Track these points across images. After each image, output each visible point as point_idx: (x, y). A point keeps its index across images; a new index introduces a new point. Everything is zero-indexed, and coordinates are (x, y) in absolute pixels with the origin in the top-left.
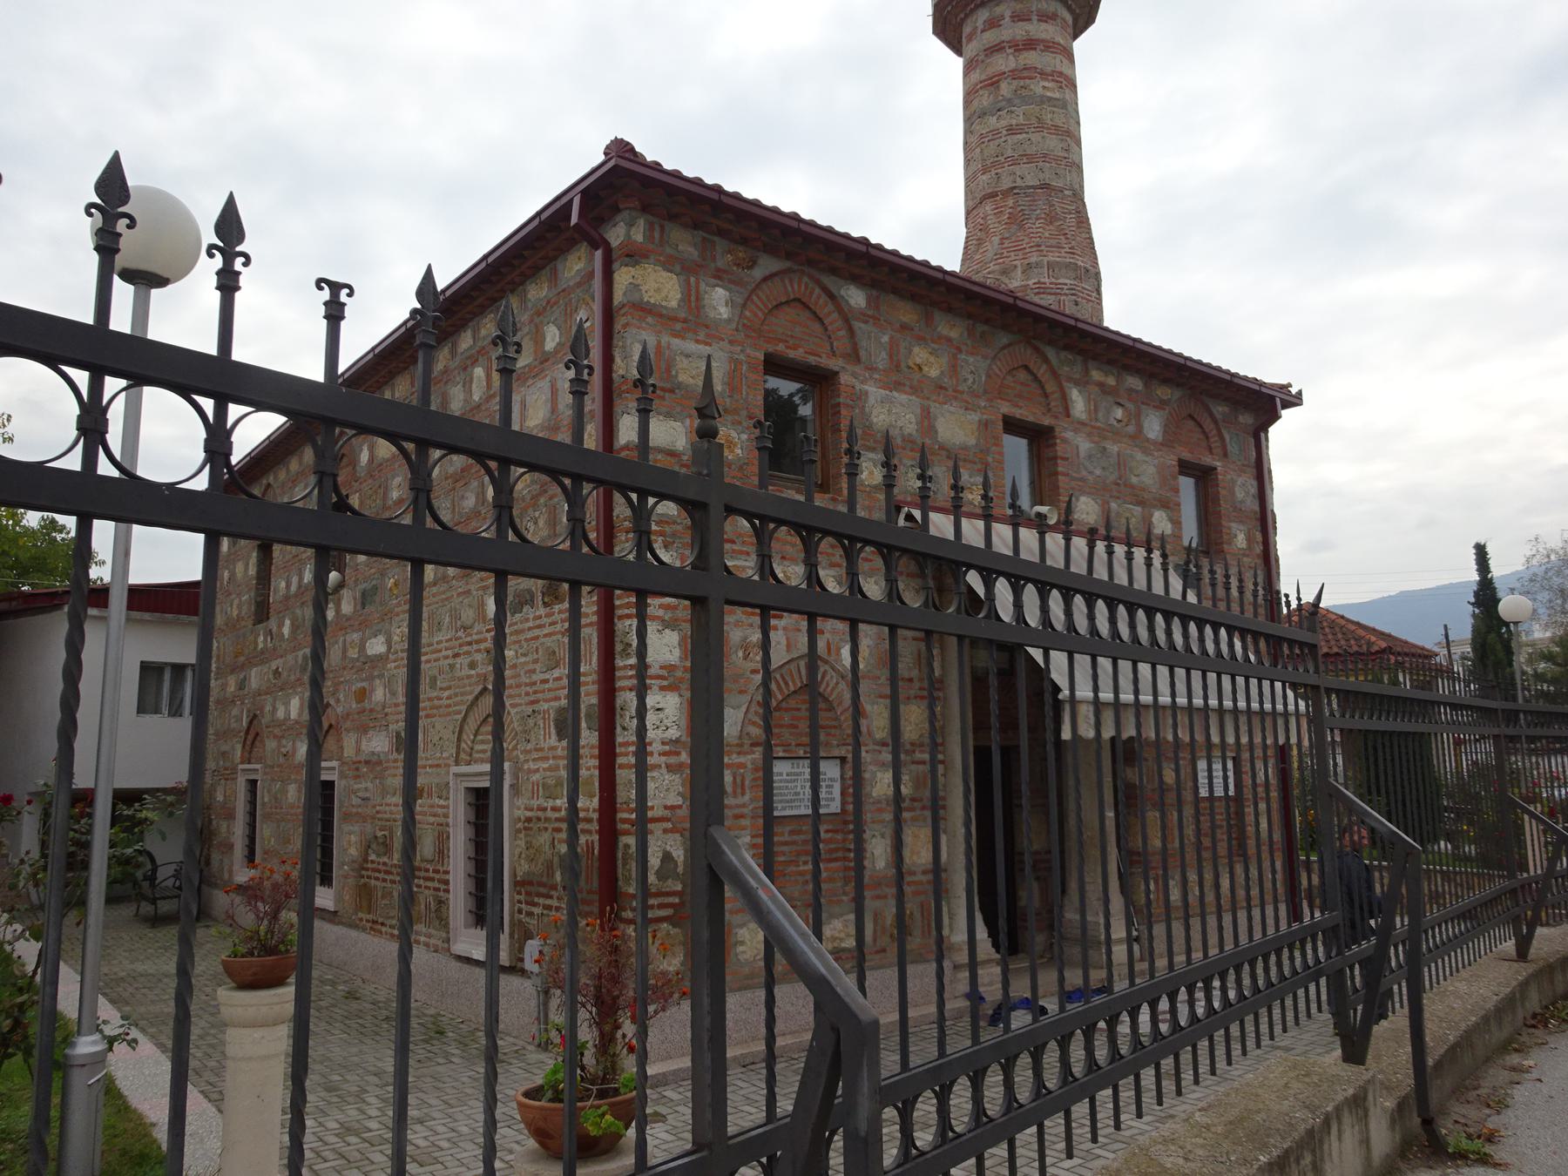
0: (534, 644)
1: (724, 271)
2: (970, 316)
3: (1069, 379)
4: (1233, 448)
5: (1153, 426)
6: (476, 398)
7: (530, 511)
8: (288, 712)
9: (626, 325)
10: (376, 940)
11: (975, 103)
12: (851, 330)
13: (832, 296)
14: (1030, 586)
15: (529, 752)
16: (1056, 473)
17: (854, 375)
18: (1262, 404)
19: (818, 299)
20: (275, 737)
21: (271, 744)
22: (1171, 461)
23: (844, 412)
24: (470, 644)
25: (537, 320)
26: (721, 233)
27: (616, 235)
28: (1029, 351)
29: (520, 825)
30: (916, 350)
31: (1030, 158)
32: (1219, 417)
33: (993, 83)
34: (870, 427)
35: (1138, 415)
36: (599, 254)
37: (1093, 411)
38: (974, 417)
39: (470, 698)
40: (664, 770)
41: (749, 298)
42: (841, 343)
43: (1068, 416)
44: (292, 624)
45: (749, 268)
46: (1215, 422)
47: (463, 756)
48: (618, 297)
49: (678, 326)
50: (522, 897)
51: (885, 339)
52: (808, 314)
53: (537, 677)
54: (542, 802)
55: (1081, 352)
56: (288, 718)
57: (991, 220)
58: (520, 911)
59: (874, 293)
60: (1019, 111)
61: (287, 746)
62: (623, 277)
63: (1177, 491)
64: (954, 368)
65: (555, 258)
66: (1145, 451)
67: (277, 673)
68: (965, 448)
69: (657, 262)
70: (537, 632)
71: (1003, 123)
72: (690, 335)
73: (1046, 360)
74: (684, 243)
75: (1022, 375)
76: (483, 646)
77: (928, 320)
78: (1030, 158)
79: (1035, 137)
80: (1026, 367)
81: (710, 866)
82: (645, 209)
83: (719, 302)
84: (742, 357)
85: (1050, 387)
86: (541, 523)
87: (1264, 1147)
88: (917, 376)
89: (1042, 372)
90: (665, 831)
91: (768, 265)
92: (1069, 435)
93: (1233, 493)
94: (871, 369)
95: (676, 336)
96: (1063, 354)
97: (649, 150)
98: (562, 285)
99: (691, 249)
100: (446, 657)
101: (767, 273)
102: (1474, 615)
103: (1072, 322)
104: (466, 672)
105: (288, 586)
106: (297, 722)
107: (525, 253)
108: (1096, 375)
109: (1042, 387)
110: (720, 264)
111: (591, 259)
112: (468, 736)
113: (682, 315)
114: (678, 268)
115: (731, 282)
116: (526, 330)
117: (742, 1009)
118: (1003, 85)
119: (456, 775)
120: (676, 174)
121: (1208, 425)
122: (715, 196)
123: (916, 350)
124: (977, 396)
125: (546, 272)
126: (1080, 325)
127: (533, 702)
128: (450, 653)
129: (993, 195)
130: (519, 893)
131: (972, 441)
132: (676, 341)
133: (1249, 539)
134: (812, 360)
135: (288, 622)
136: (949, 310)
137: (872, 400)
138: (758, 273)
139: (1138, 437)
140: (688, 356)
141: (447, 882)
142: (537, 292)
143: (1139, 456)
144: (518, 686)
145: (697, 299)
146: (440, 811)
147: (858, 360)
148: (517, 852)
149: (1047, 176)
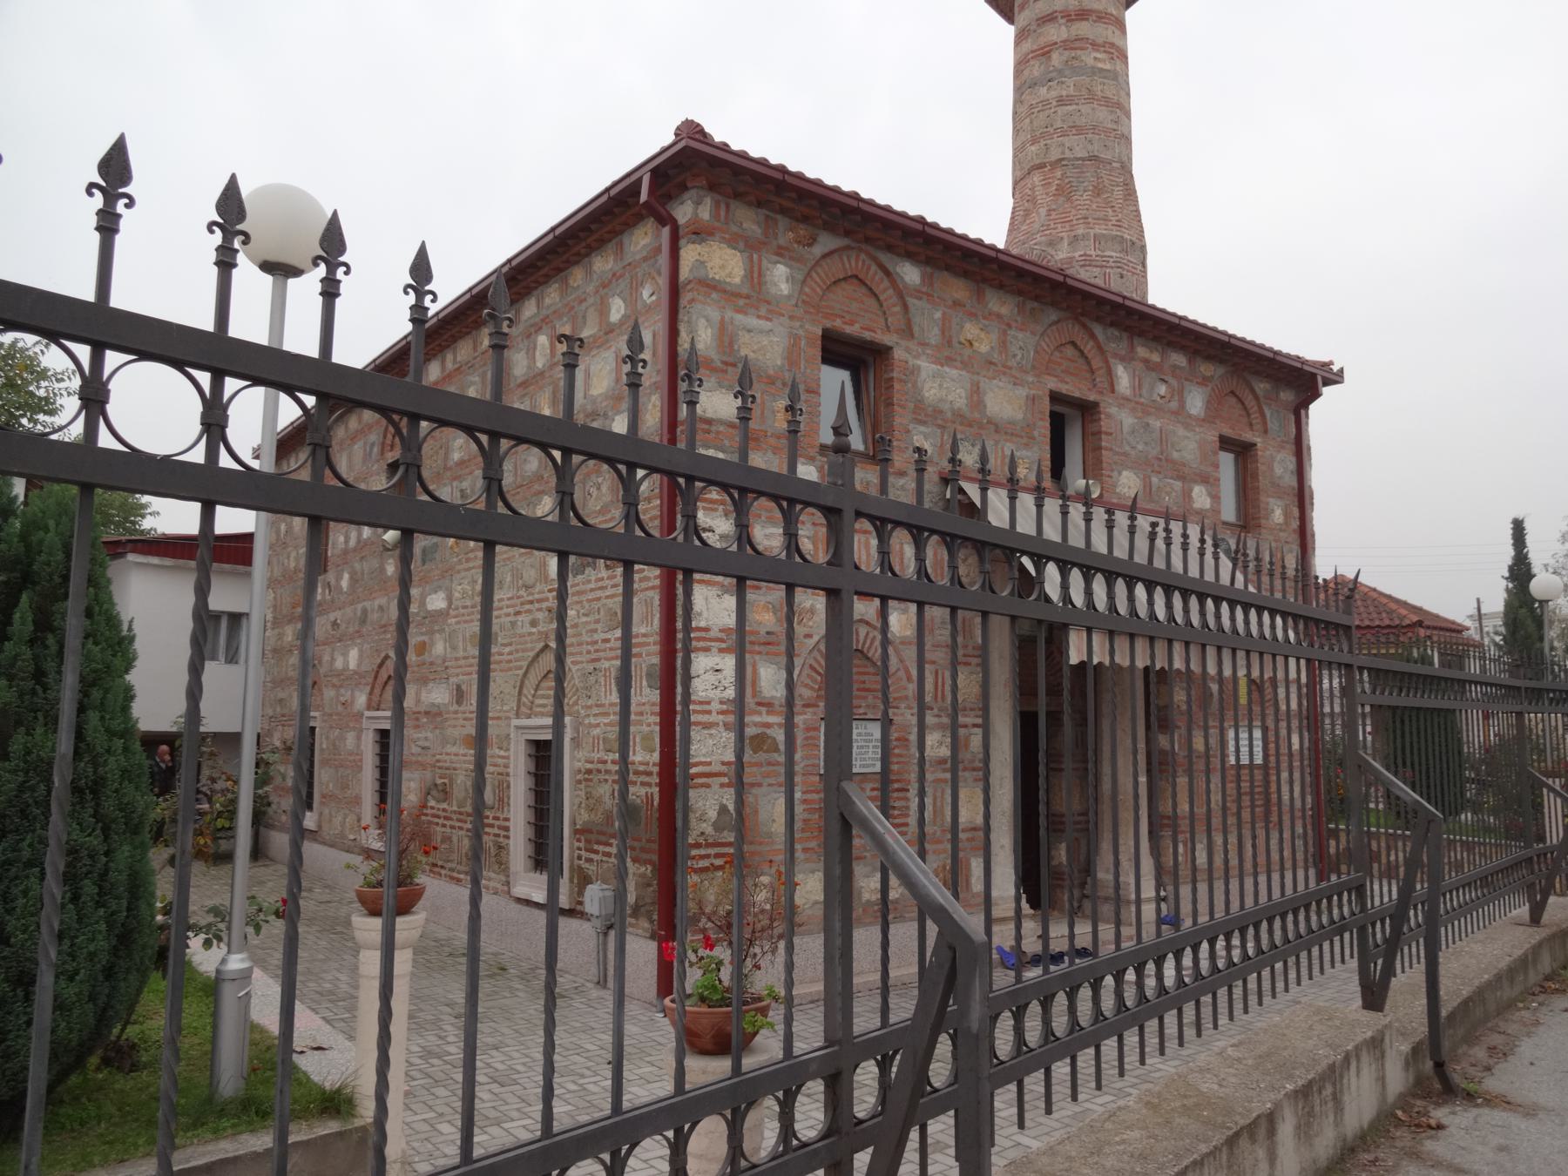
0: (596, 605)
1: (787, 249)
2: (1020, 293)
3: (1116, 356)
4: (1273, 425)
5: (1196, 402)
6: (539, 364)
7: (593, 477)
8: (346, 663)
9: (693, 300)
10: (436, 882)
11: (1026, 73)
12: (905, 307)
13: (887, 273)
14: (1099, 576)
15: (590, 707)
16: (1100, 448)
17: (908, 350)
18: (1302, 381)
19: (874, 275)
20: (334, 686)
21: (329, 693)
22: (1212, 437)
23: (897, 386)
24: (531, 602)
25: (602, 292)
26: (783, 211)
27: (683, 212)
28: (1077, 327)
29: (579, 777)
30: (968, 326)
31: (1079, 130)
32: (1260, 393)
33: (1045, 53)
34: (921, 401)
35: (1181, 393)
36: (666, 231)
37: (1137, 387)
38: (1022, 392)
39: (532, 654)
40: (721, 729)
41: (808, 274)
42: (896, 319)
43: (1113, 391)
44: (351, 578)
45: (810, 245)
46: (1256, 398)
47: (523, 709)
48: (685, 273)
49: (741, 302)
50: (582, 845)
51: (938, 315)
52: (864, 289)
53: (599, 636)
54: (602, 755)
55: (1127, 329)
56: (346, 668)
57: (1039, 191)
58: (579, 858)
59: (929, 270)
60: (1070, 82)
61: (346, 695)
62: (690, 254)
63: (1217, 466)
64: (1003, 344)
65: (622, 232)
66: (1187, 426)
67: (335, 624)
68: (1011, 423)
69: (723, 240)
70: (599, 594)
71: (1054, 94)
72: (752, 311)
73: (1093, 336)
74: (748, 220)
75: (1070, 352)
76: (544, 605)
77: (980, 295)
78: (1079, 130)
79: (1085, 109)
80: (1073, 344)
81: (842, 815)
82: (712, 187)
83: (780, 278)
84: (801, 332)
85: (1097, 363)
86: (604, 489)
87: (1290, 1077)
88: (967, 352)
89: (1089, 348)
90: (722, 785)
91: (827, 242)
92: (1113, 410)
93: (1271, 469)
94: (923, 344)
95: (738, 311)
97: (719, 132)
98: (628, 259)
99: (754, 227)
100: (508, 615)
101: (826, 250)
102: (1507, 590)
103: (1120, 300)
104: (528, 629)
105: (347, 541)
106: (355, 672)
107: (593, 227)
108: (1142, 351)
109: (1088, 363)
110: (782, 241)
111: (658, 236)
112: (529, 690)
113: (745, 291)
114: (741, 245)
115: (791, 258)
116: (591, 300)
117: (865, 940)
118: (1055, 55)
119: (518, 728)
120: (743, 155)
121: (1250, 401)
122: (779, 176)
123: (968, 326)
124: (1026, 372)
125: (611, 246)
126: (1128, 303)
127: (594, 660)
128: (511, 610)
129: (1041, 166)
130: (579, 840)
131: (1020, 416)
132: (739, 317)
133: (1286, 514)
134: (867, 335)
135: (346, 576)
136: (1001, 287)
137: (923, 374)
138: (817, 250)
139: (1180, 413)
140: (749, 331)
141: (507, 829)
142: (603, 264)
143: (1181, 431)
144: (580, 644)
145: (760, 275)
146: (500, 761)
147: (912, 336)
148: (577, 801)
149: (1096, 148)
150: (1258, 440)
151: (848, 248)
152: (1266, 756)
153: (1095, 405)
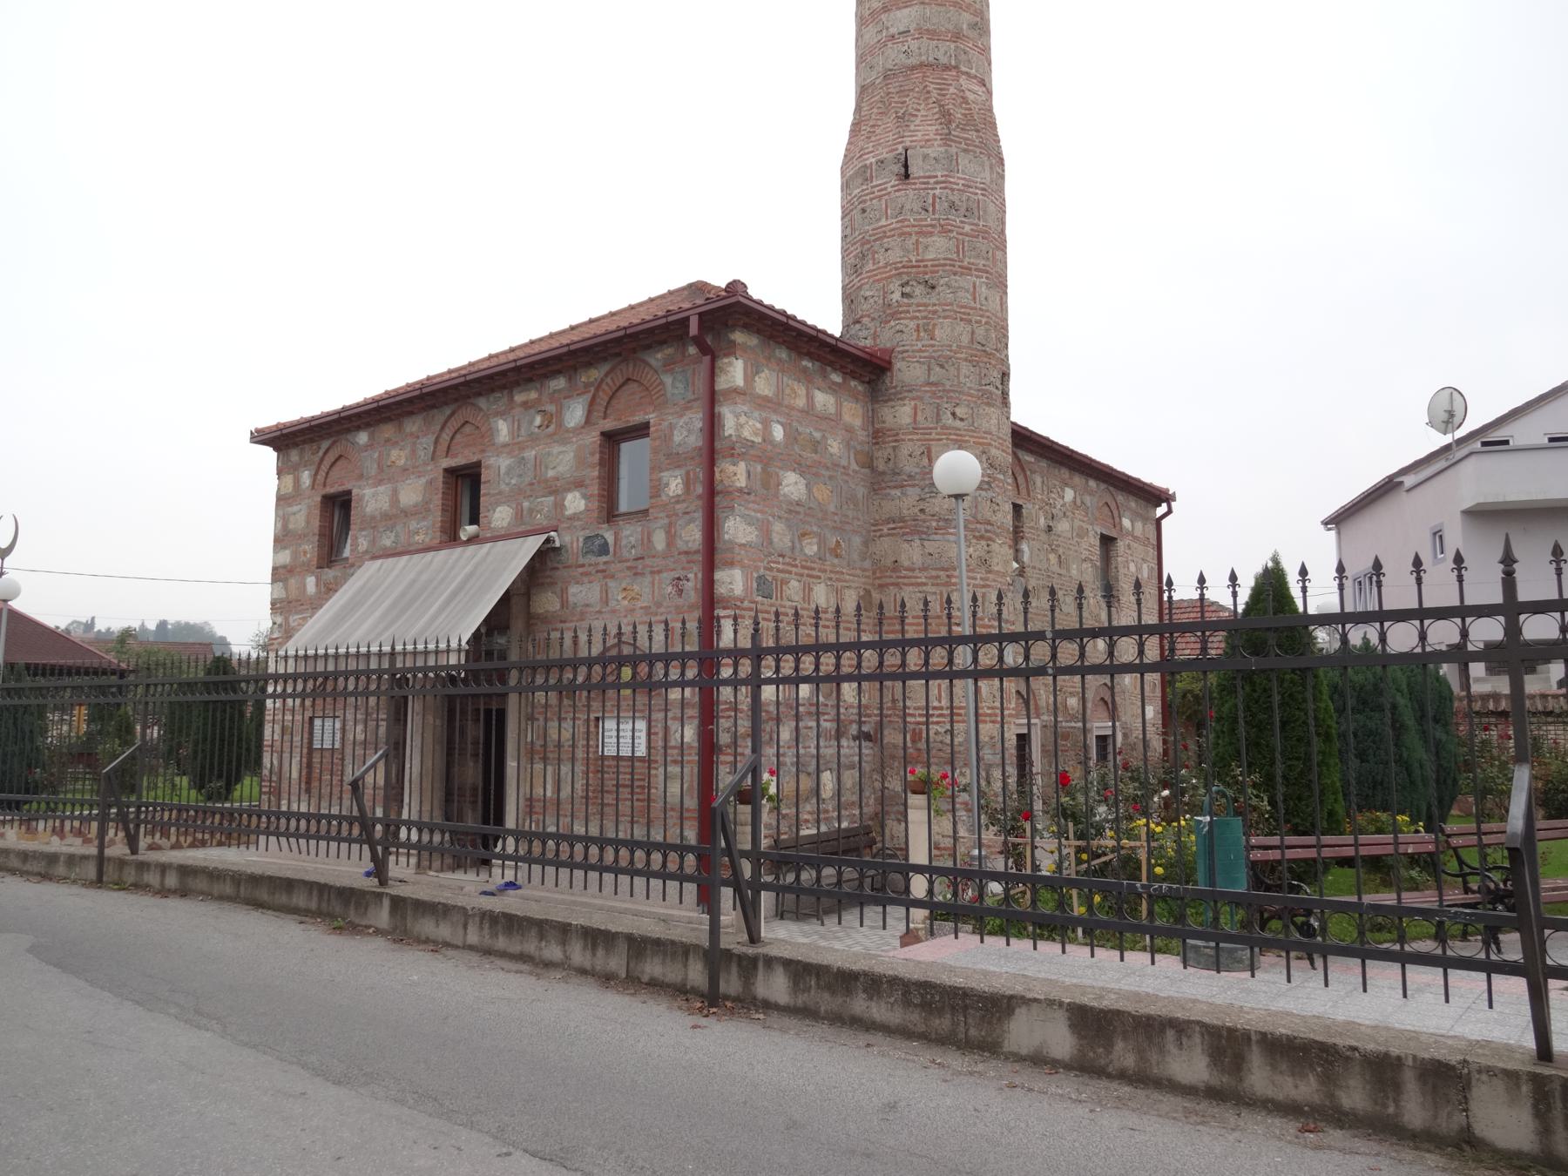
22: (592, 438)
26: (304, 442)
55: (504, 387)
64: (414, 452)
66: (564, 442)
75: (468, 429)
77: (400, 428)
91: (325, 444)
92: (492, 461)
108: (519, 398)
133: (687, 484)
134: (341, 489)
143: (556, 449)
150: (652, 417)
151: (334, 443)
152: (649, 747)
153: (478, 464)
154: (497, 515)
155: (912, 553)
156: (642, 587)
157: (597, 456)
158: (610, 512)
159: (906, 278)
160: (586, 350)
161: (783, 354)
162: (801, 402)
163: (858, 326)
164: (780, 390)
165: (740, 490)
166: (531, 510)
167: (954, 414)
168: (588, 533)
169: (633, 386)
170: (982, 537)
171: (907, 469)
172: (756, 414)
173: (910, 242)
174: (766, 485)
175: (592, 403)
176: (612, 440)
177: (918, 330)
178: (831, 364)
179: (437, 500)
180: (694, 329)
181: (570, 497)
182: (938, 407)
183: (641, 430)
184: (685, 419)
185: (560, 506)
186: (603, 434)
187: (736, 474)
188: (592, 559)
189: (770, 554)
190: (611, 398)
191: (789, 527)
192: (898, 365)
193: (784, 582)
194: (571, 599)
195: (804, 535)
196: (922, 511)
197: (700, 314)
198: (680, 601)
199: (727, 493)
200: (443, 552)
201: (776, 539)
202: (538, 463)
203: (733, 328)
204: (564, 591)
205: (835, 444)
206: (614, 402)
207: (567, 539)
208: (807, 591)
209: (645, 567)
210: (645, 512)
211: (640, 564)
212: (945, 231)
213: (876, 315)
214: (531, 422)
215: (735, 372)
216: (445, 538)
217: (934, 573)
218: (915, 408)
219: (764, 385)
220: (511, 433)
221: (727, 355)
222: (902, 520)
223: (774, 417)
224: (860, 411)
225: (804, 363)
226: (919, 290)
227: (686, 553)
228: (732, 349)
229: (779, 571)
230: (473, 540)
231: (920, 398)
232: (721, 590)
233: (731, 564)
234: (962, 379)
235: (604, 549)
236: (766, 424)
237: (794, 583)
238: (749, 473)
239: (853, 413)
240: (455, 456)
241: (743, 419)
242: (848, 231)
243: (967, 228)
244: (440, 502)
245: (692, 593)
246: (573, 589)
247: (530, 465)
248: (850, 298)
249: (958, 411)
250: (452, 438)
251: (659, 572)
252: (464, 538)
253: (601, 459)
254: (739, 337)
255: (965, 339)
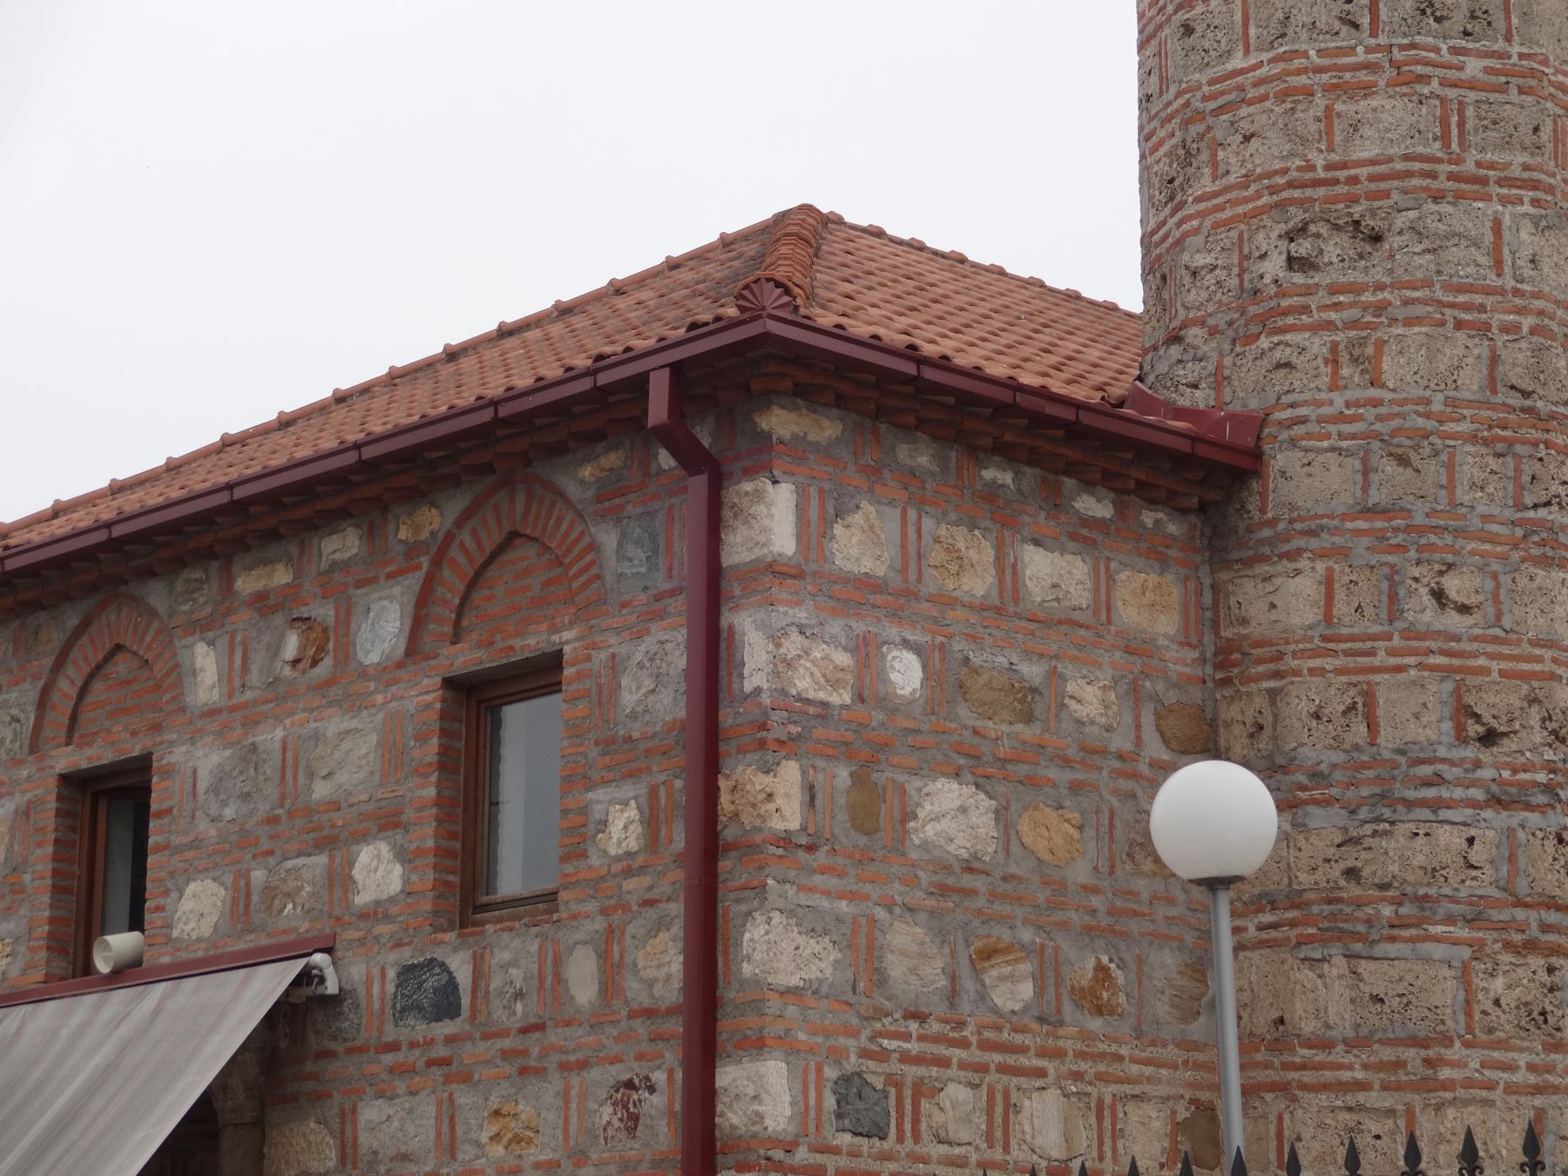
22: (421, 695)
66: (353, 704)
73: (153, 614)
75: (122, 667)
92: (177, 755)
96: (179, 586)
108: (247, 584)
133: (652, 822)
143: (335, 723)
150: (568, 639)
153: (143, 765)
154: (186, 905)
155: (1325, 996)
156: (538, 1105)
157: (435, 742)
158: (465, 888)
159: (1297, 216)
160: (408, 458)
161: (920, 456)
162: (979, 583)
163: (1175, 351)
164: (910, 556)
165: (785, 840)
166: (270, 891)
167: (1439, 595)
168: (407, 956)
169: (525, 554)
170: (1531, 946)
171: (1308, 755)
172: (835, 627)
173: (1308, 117)
174: (865, 821)
175: (423, 600)
176: (476, 701)
177: (1333, 361)
178: (1071, 469)
179: (41, 861)
180: (658, 409)
181: (365, 855)
182: (1393, 575)
183: (540, 675)
184: (649, 644)
185: (339, 880)
186: (450, 683)
187: (773, 795)
188: (419, 1029)
189: (879, 1013)
190: (473, 584)
191: (942, 936)
192: (1280, 459)
193: (921, 1090)
194: (363, 1138)
195: (988, 954)
196: (1352, 873)
197: (676, 368)
198: (632, 1149)
199: (748, 848)
200: (50, 1006)
201: (896, 969)
202: (293, 762)
203: (766, 399)
204: (348, 1116)
205: (1091, 693)
206: (478, 595)
207: (357, 972)
208: (1001, 1116)
209: (546, 1051)
210: (550, 897)
211: (534, 1042)
212: (1406, 80)
213: (1219, 320)
214: (275, 650)
215: (771, 518)
216: (61, 966)
217: (1388, 1054)
218: (1329, 581)
219: (862, 544)
220: (226, 677)
221: (750, 472)
222: (1296, 900)
223: (893, 631)
224: (1176, 593)
225: (989, 474)
226: (1335, 247)
227: (649, 1013)
228: (762, 458)
229: (906, 1058)
230: (128, 973)
231: (1343, 553)
232: (731, 1118)
233: (757, 1045)
234: (1463, 495)
235: (446, 1004)
236: (867, 653)
237: (957, 1093)
238: (811, 792)
239: (1150, 603)
240: (87, 742)
241: (792, 645)
242: (1153, 86)
243: (1473, 67)
244: (46, 867)
245: (662, 1126)
246: (371, 1112)
247: (271, 768)
248: (1158, 266)
249: (1454, 585)
250: (83, 691)
251: (583, 1065)
252: (103, 967)
253: (444, 751)
254: (780, 422)
255: (1471, 381)
